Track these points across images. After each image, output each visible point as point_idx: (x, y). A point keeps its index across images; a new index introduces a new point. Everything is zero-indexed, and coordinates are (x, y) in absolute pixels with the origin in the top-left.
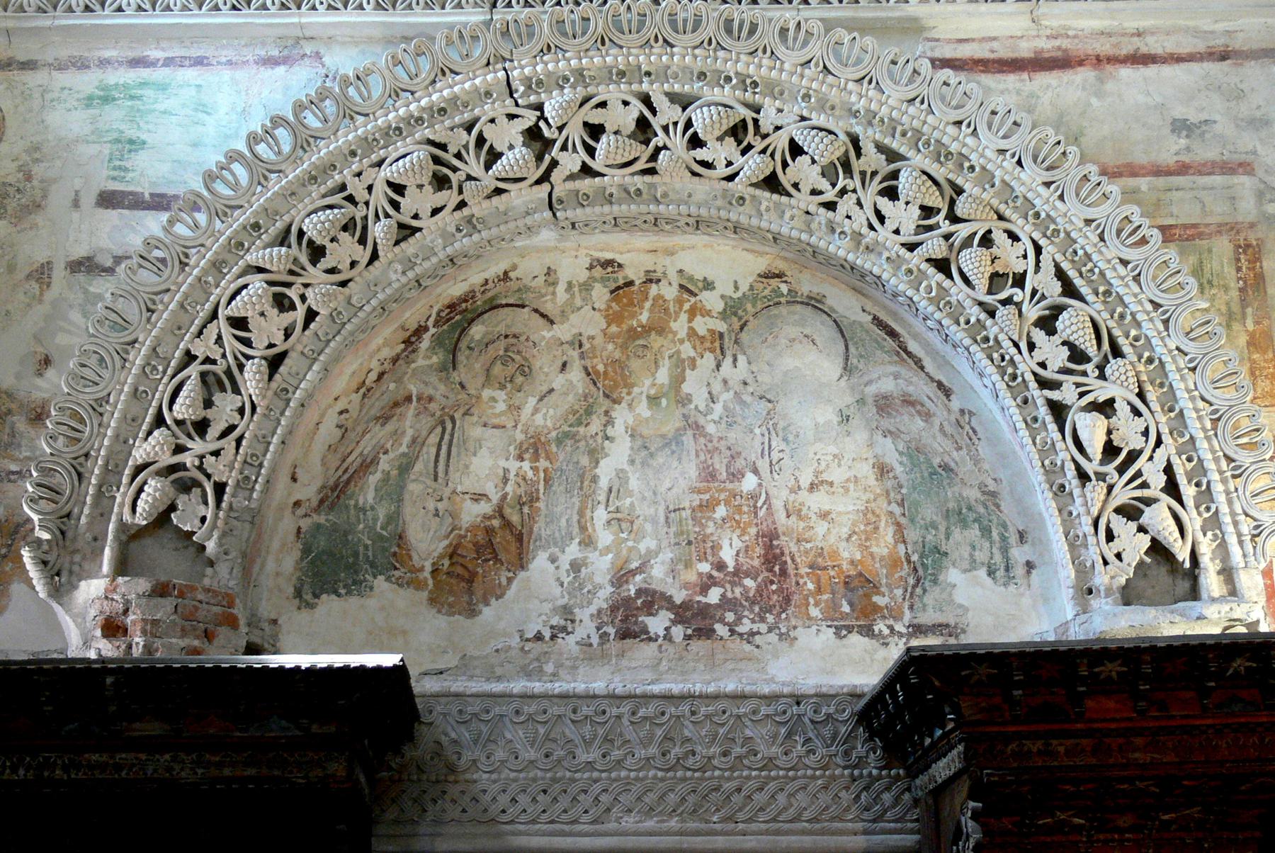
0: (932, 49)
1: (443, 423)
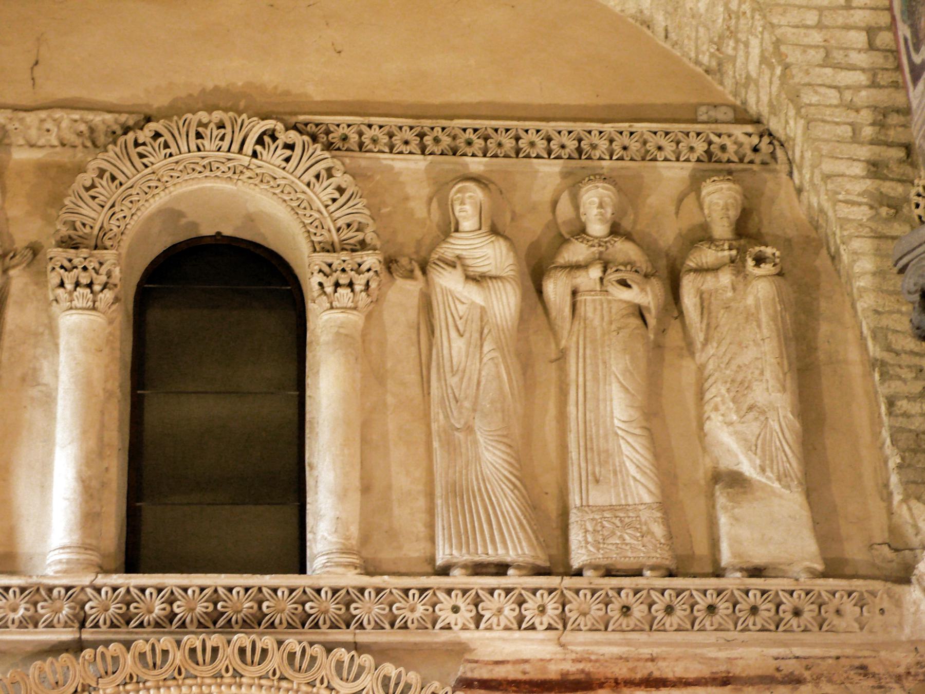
0: (472, 670)
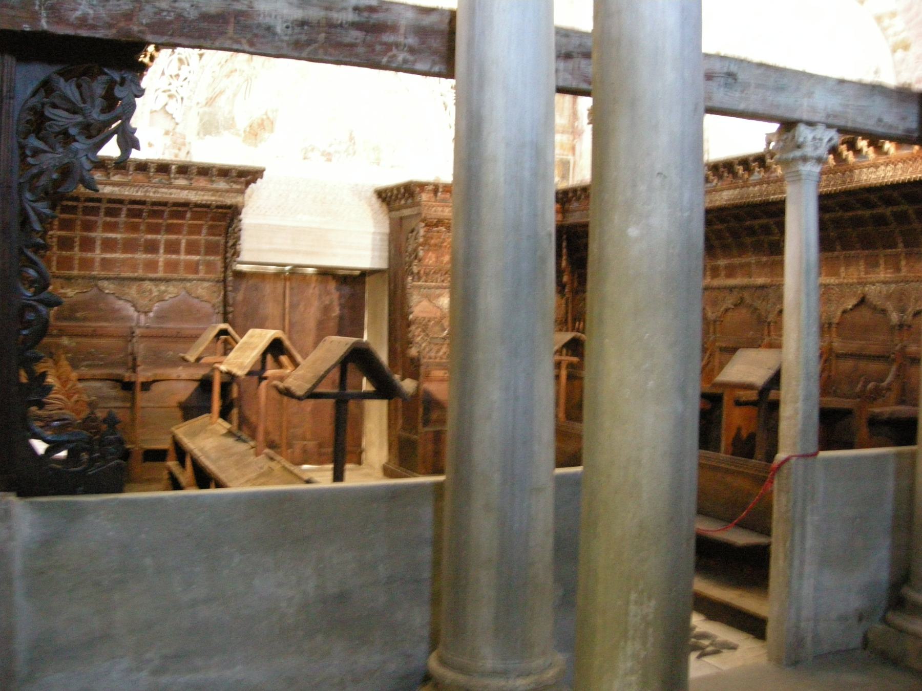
1: (247, 80)
